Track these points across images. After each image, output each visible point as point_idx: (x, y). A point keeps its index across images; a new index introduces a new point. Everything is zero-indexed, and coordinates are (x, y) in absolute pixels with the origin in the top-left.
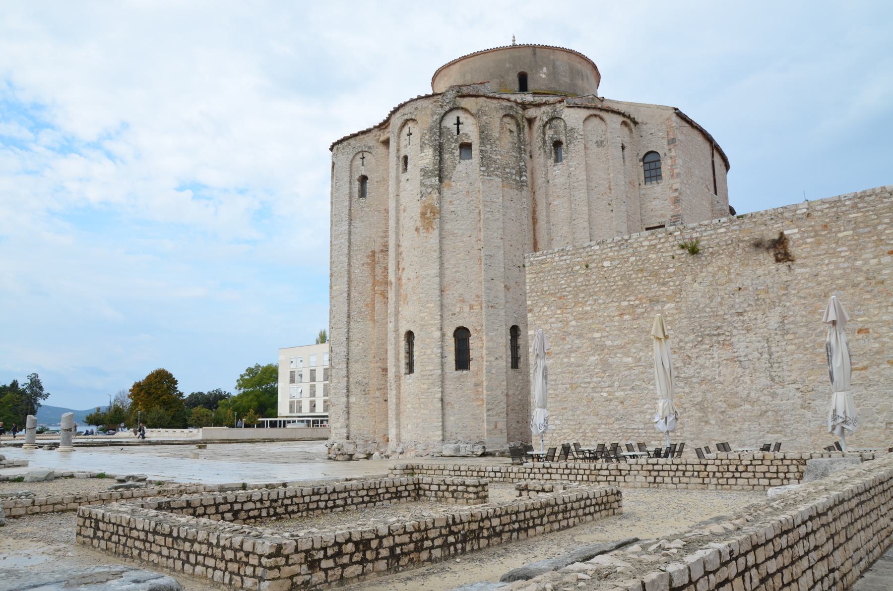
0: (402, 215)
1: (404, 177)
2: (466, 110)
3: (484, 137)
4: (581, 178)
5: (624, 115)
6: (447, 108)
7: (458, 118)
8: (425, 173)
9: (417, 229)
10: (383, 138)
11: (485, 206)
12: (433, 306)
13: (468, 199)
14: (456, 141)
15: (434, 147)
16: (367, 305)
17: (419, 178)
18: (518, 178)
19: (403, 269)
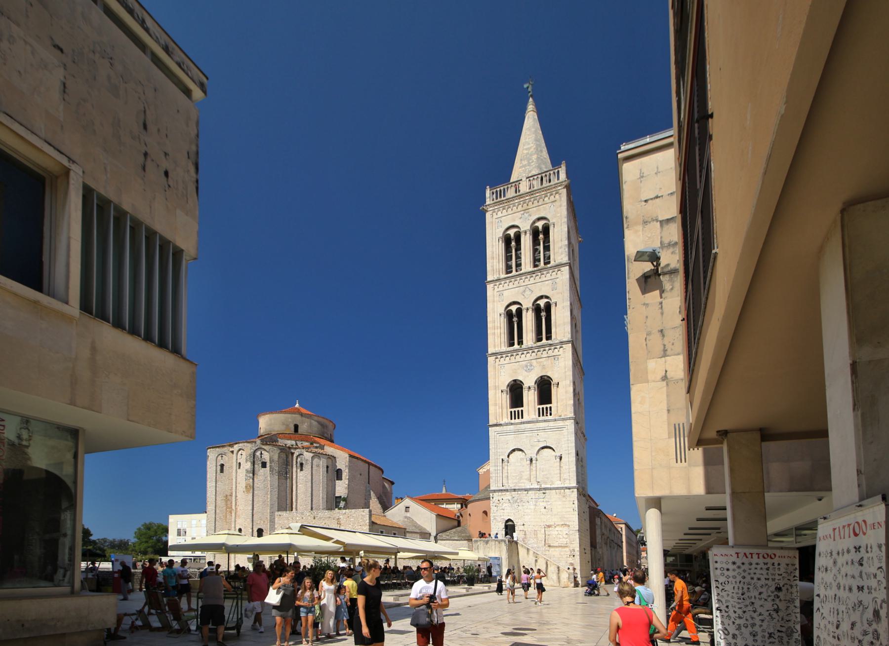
0: (238, 485)
1: (238, 470)
2: (265, 450)
3: (271, 461)
5: (329, 455)
6: (257, 448)
7: (261, 452)
8: (247, 471)
9: (244, 492)
10: (231, 449)
11: (271, 486)
12: (250, 520)
13: (264, 483)
14: (260, 461)
15: (251, 462)
16: (223, 516)
17: (245, 473)
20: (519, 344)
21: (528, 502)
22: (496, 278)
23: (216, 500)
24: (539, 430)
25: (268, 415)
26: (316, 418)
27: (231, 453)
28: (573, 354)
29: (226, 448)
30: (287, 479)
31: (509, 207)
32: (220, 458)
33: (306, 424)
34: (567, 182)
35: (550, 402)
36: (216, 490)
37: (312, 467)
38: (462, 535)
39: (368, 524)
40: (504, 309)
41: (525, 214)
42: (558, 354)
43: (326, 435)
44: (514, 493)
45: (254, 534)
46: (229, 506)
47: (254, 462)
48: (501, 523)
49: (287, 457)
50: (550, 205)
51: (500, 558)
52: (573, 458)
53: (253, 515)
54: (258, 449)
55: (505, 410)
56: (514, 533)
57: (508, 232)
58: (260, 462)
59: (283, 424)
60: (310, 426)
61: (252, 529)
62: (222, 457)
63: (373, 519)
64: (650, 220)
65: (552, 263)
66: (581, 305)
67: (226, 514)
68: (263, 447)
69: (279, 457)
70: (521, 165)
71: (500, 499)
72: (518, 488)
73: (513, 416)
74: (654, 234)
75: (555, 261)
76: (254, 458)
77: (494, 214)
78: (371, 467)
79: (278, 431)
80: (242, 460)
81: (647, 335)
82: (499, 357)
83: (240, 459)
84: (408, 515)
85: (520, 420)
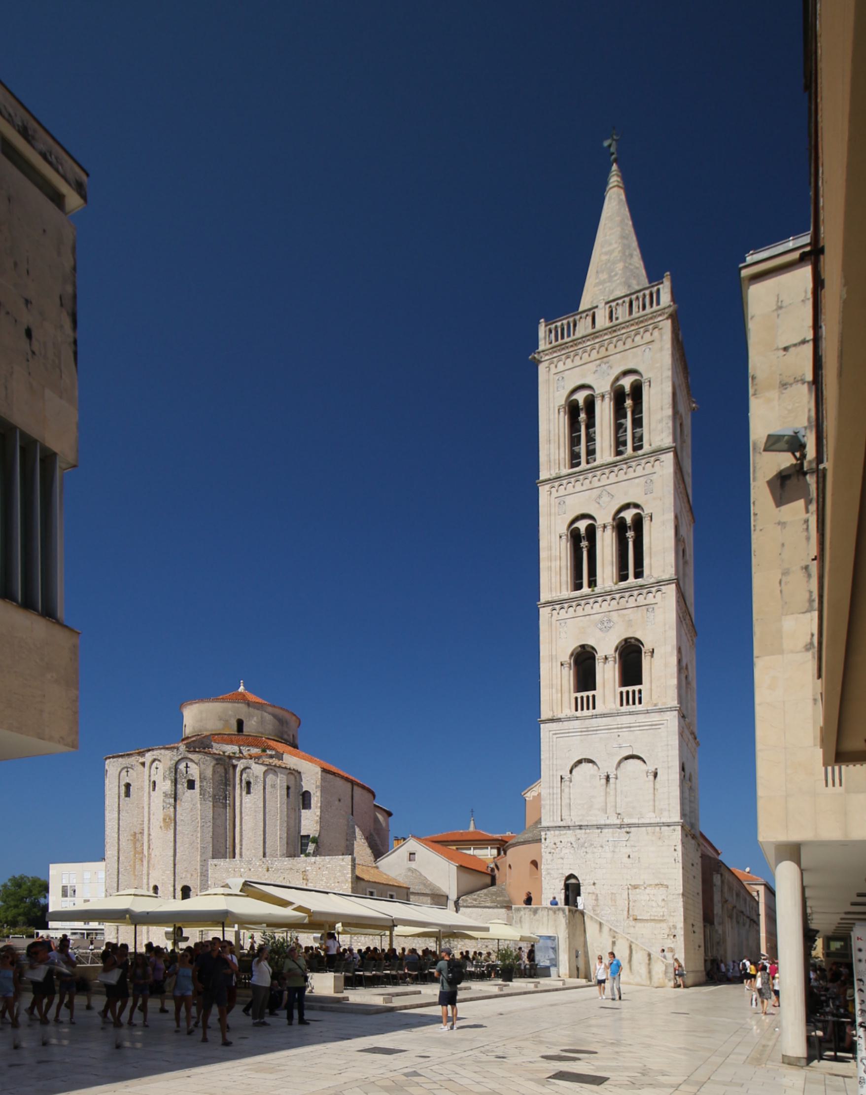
0: (152, 816)
2: (192, 760)
3: (202, 778)
4: (260, 806)
6: (180, 757)
7: (187, 764)
8: (166, 795)
9: (161, 827)
11: (201, 819)
14: (185, 778)
16: (131, 865)
17: (162, 798)
18: (224, 801)
19: (153, 849)
20: (590, 586)
21: (602, 847)
22: (554, 475)
23: (119, 839)
24: (621, 728)
25: (197, 705)
26: (270, 709)
27: (141, 766)
28: (678, 602)
29: (133, 758)
30: (226, 806)
31: (577, 355)
32: (124, 773)
33: (255, 719)
34: (671, 309)
35: (640, 682)
36: (119, 825)
37: (264, 788)
38: (498, 899)
39: (350, 880)
40: (566, 526)
41: (603, 366)
42: (654, 601)
43: (285, 737)
44: (578, 831)
45: (177, 895)
46: (139, 849)
47: (176, 780)
48: (557, 880)
49: (226, 772)
50: (643, 348)
51: (555, 937)
52: (674, 775)
53: (175, 865)
54: (182, 759)
55: (566, 696)
56: (578, 898)
57: (575, 397)
58: (185, 780)
59: (220, 719)
60: (262, 721)
61: (174, 886)
62: (127, 771)
63: (358, 873)
64: (791, 380)
65: (646, 448)
66: (693, 518)
67: (135, 862)
68: (190, 756)
69: (214, 772)
70: (597, 281)
71: (557, 841)
72: (586, 823)
73: (579, 705)
74: (797, 405)
75: (650, 445)
76: (176, 774)
77: (552, 366)
78: (355, 788)
79: (212, 731)
80: (158, 777)
81: (783, 574)
82: (557, 607)
83: (155, 775)
84: (413, 865)
85: (591, 712)
